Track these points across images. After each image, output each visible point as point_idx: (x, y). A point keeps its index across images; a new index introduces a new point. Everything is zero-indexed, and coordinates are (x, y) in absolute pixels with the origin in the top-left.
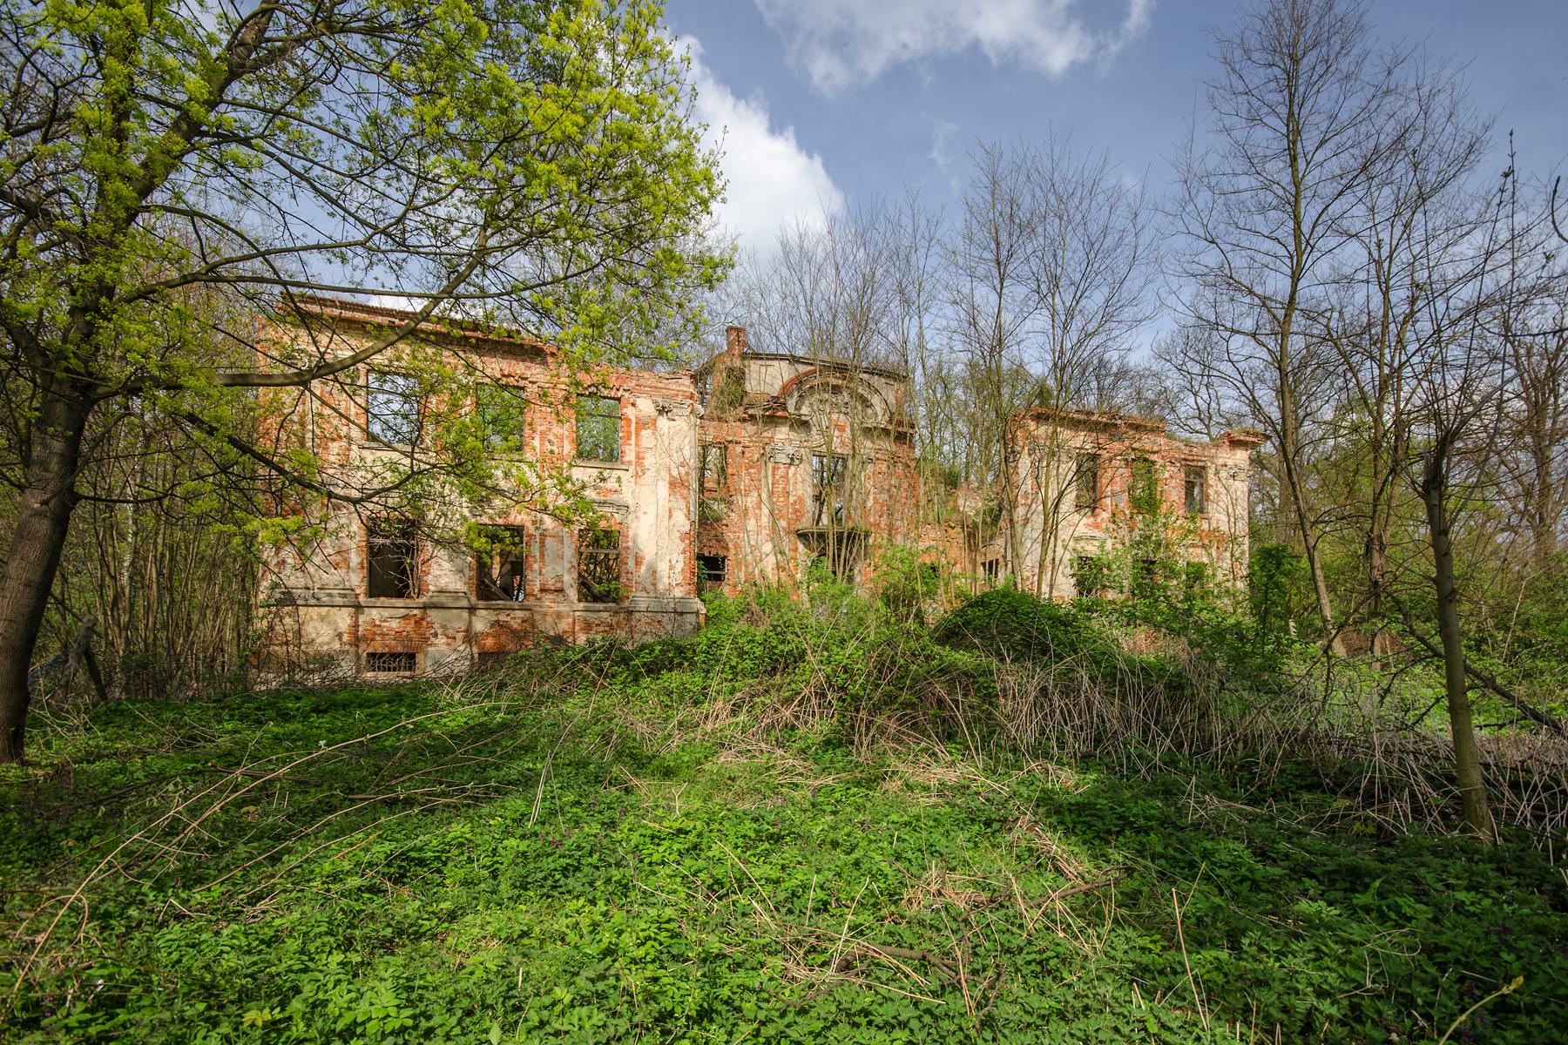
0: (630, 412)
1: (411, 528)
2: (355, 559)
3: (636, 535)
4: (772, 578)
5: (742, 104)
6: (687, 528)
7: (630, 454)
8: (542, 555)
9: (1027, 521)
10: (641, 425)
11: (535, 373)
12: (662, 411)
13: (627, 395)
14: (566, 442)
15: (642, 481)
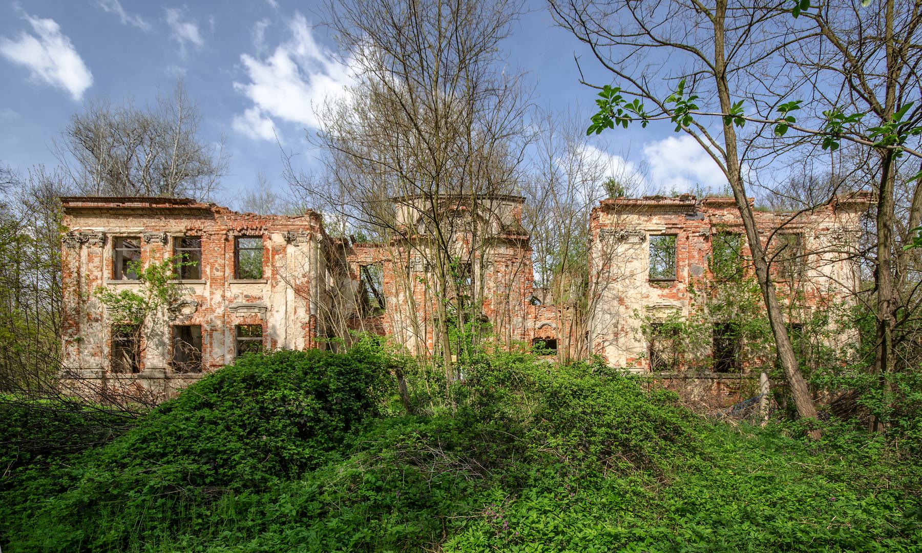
0: (268, 244)
1: (137, 327)
2: (107, 350)
3: (274, 327)
4: (414, 354)
5: (297, 74)
6: (307, 320)
7: (268, 272)
8: (211, 344)
9: (168, 462)
10: (276, 251)
11: (207, 226)
12: (289, 241)
13: (266, 232)
14: (227, 268)
15: (275, 290)
